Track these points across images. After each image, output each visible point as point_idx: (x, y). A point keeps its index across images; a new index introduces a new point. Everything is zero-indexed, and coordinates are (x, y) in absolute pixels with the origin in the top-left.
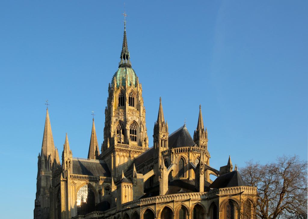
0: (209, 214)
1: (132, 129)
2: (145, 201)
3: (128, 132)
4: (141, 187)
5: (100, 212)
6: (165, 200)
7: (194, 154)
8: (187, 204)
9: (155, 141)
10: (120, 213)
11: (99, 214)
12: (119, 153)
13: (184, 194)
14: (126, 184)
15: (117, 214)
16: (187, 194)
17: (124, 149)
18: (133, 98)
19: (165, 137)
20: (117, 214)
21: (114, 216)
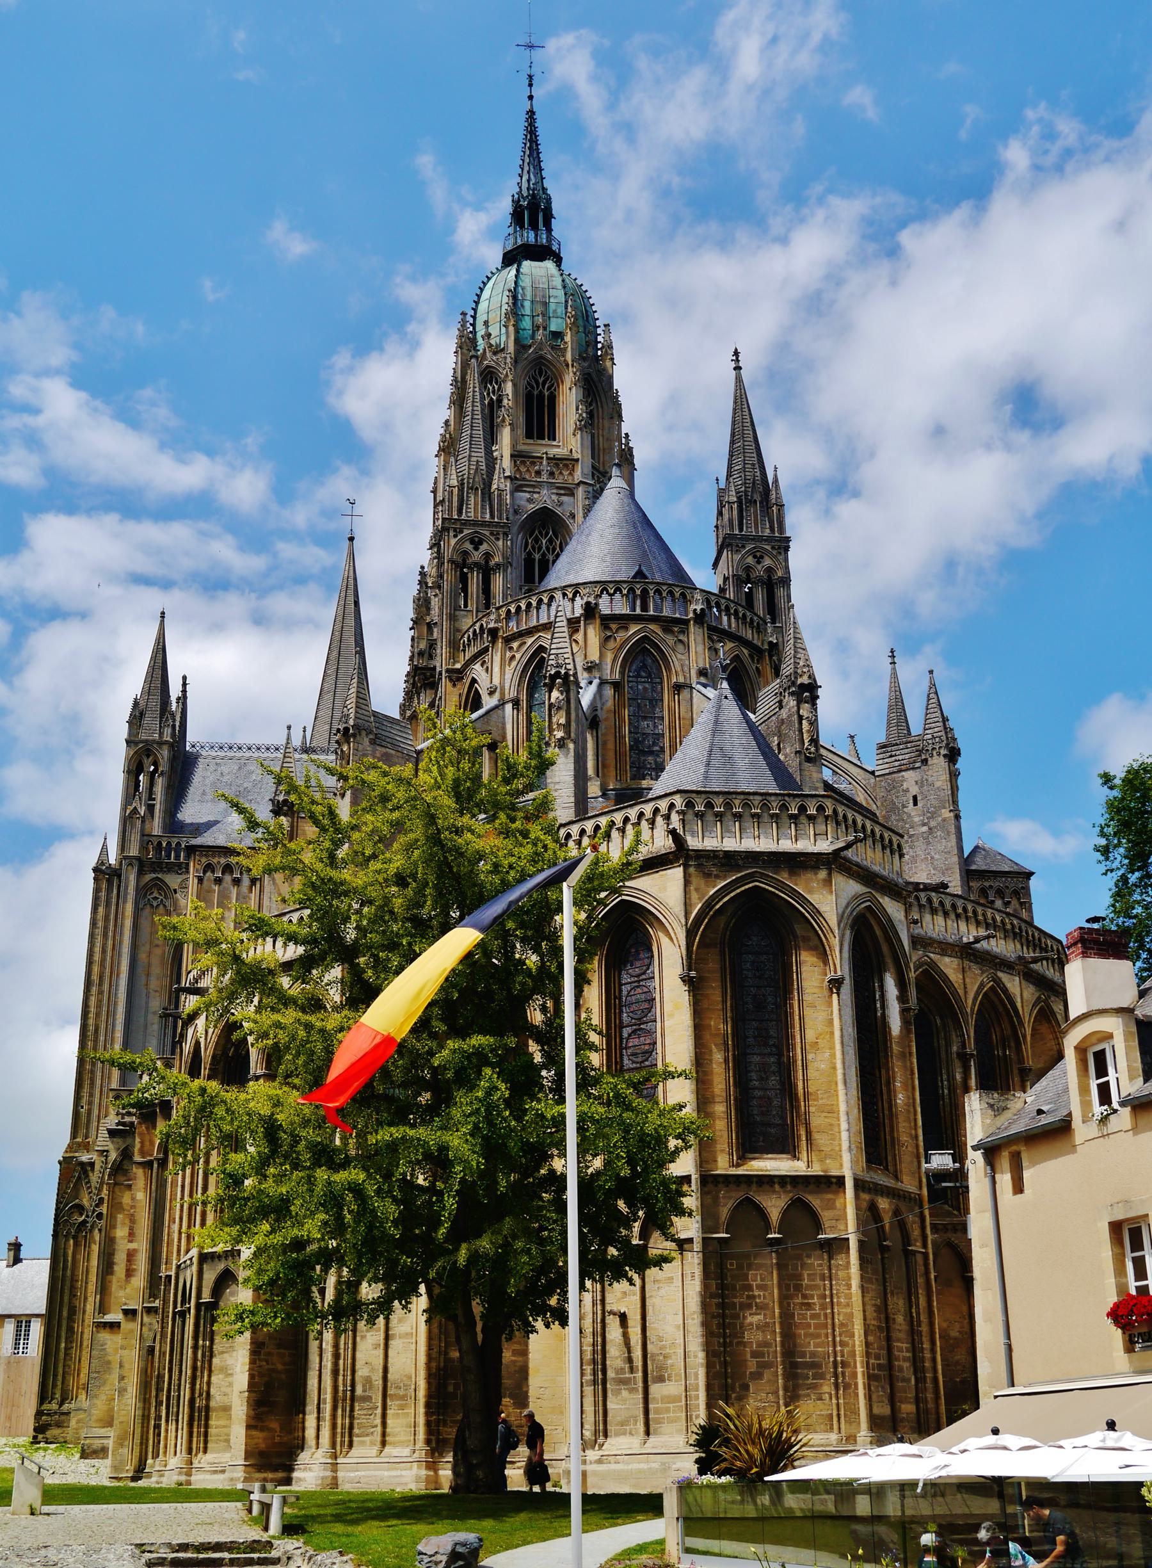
1: (537, 556)
7: (614, 626)
19: (484, 547)
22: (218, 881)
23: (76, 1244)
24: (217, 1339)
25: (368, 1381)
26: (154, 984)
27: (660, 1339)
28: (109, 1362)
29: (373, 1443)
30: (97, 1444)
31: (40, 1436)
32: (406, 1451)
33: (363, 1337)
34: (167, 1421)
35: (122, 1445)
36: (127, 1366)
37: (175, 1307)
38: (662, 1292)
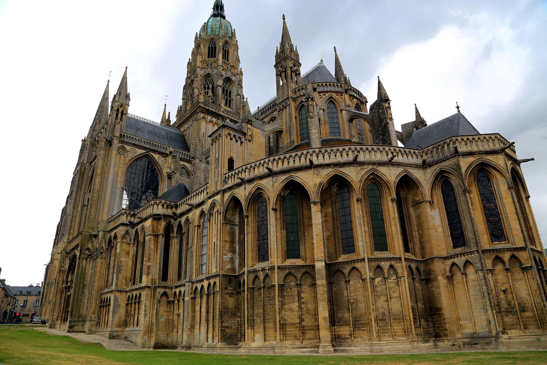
0: (433, 202)
2: (283, 162)
3: (220, 90)
4: (259, 146)
5: (168, 202)
6: (333, 159)
8: (383, 170)
9: (279, 73)
10: (218, 198)
11: (165, 206)
12: (206, 116)
13: (375, 148)
14: (233, 133)
15: (210, 201)
16: (381, 148)
17: (214, 111)
18: (228, 52)
19: (296, 67)
20: (210, 201)
21: (200, 208)
22: (231, 139)
23: (87, 262)
24: (286, 298)
25: (383, 314)
26: (119, 179)
27: (521, 298)
28: (119, 305)
29: (389, 336)
30: (115, 334)
31: (71, 330)
32: (405, 338)
33: (379, 298)
34: (248, 328)
35: (146, 335)
36: (147, 306)
37: (248, 286)
38: (519, 283)
